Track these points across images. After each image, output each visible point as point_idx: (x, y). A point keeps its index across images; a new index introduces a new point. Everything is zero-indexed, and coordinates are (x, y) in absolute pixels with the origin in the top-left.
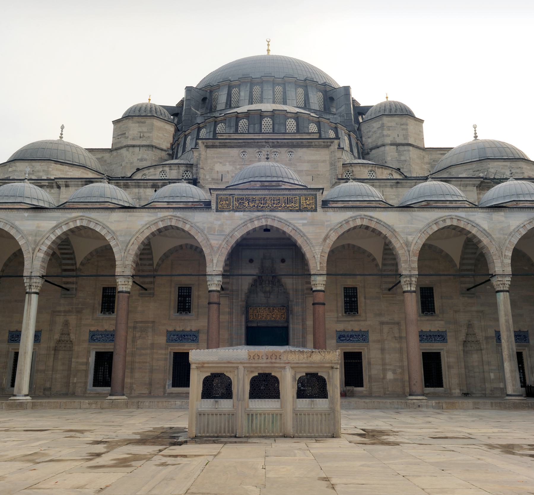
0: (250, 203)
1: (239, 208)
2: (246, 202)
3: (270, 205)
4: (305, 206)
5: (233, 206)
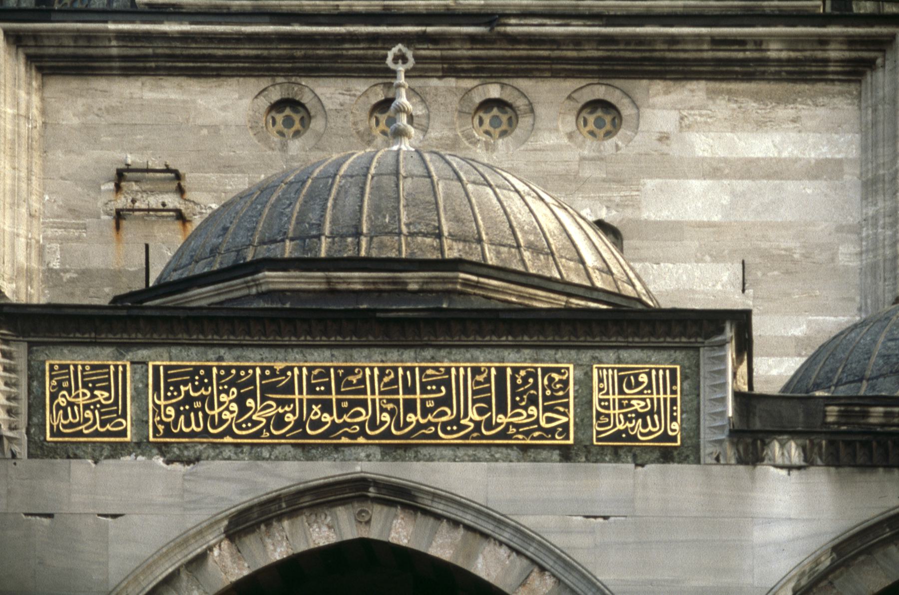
0: (250, 402)
1: (182, 434)
2: (224, 398)
3: (386, 417)
4: (620, 427)
5: (141, 423)
